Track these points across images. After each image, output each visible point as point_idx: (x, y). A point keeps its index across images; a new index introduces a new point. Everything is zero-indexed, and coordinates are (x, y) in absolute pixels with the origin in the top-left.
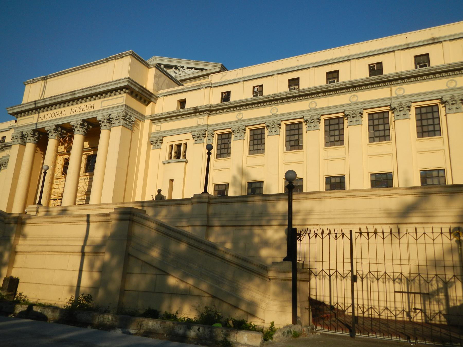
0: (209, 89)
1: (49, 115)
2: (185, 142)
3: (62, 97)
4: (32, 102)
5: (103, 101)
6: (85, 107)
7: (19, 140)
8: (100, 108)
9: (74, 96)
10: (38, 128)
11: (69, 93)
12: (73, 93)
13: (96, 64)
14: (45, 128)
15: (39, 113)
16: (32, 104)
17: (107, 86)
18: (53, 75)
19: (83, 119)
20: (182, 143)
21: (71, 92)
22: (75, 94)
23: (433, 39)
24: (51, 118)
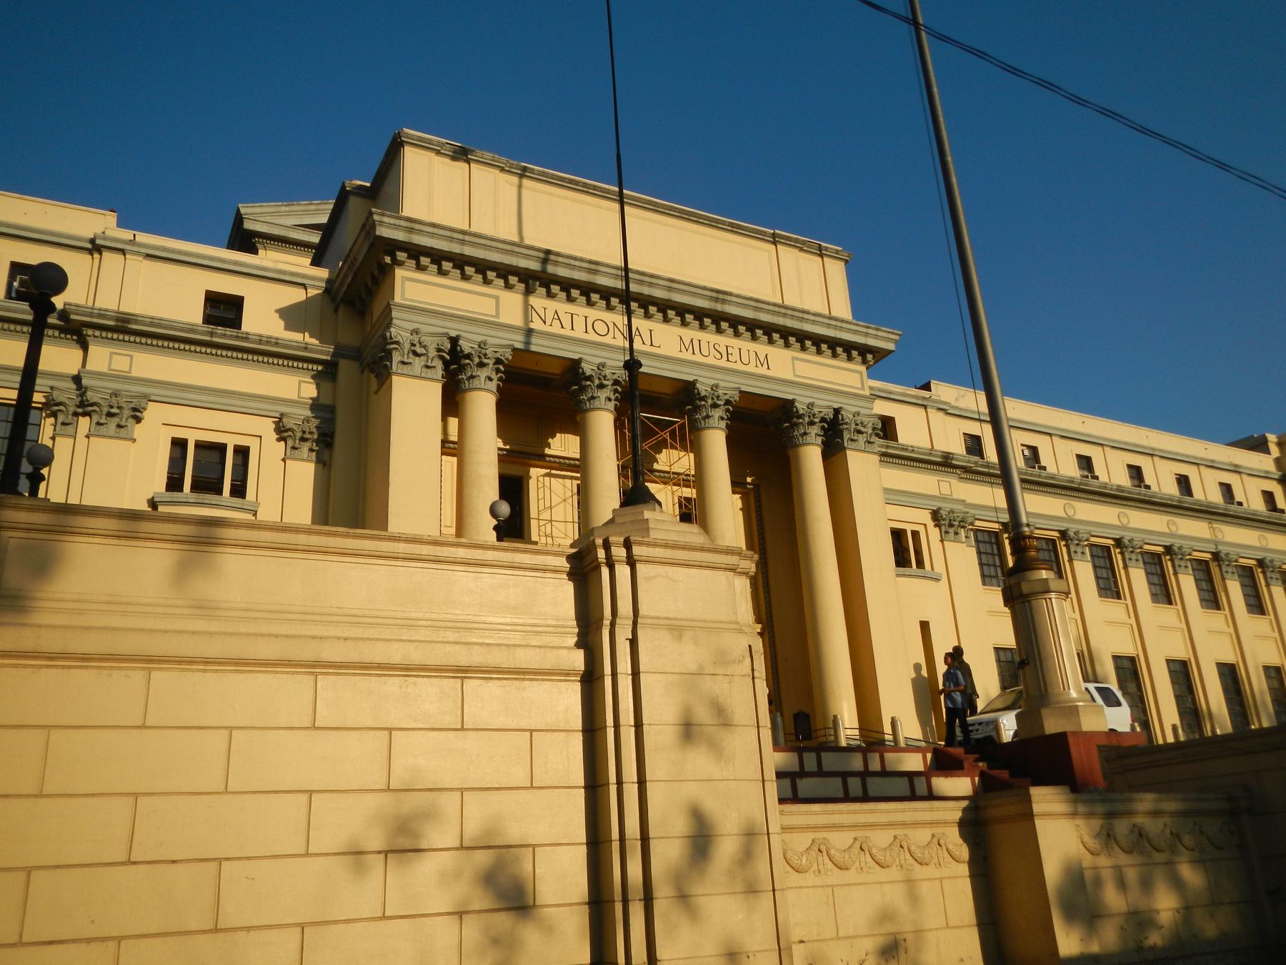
0: (941, 414)
1: (579, 323)
2: (916, 528)
3: (670, 289)
4: (539, 250)
5: (794, 359)
6: (735, 357)
7: (439, 365)
8: (790, 377)
9: (719, 307)
10: (533, 348)
11: (704, 288)
12: (720, 295)
13: (734, 229)
14: (577, 363)
15: (528, 292)
16: (527, 257)
17: (836, 327)
18: (571, 181)
19: (744, 388)
20: (909, 528)
21: (712, 290)
22: (724, 301)
23: (1236, 466)
24: (592, 337)
